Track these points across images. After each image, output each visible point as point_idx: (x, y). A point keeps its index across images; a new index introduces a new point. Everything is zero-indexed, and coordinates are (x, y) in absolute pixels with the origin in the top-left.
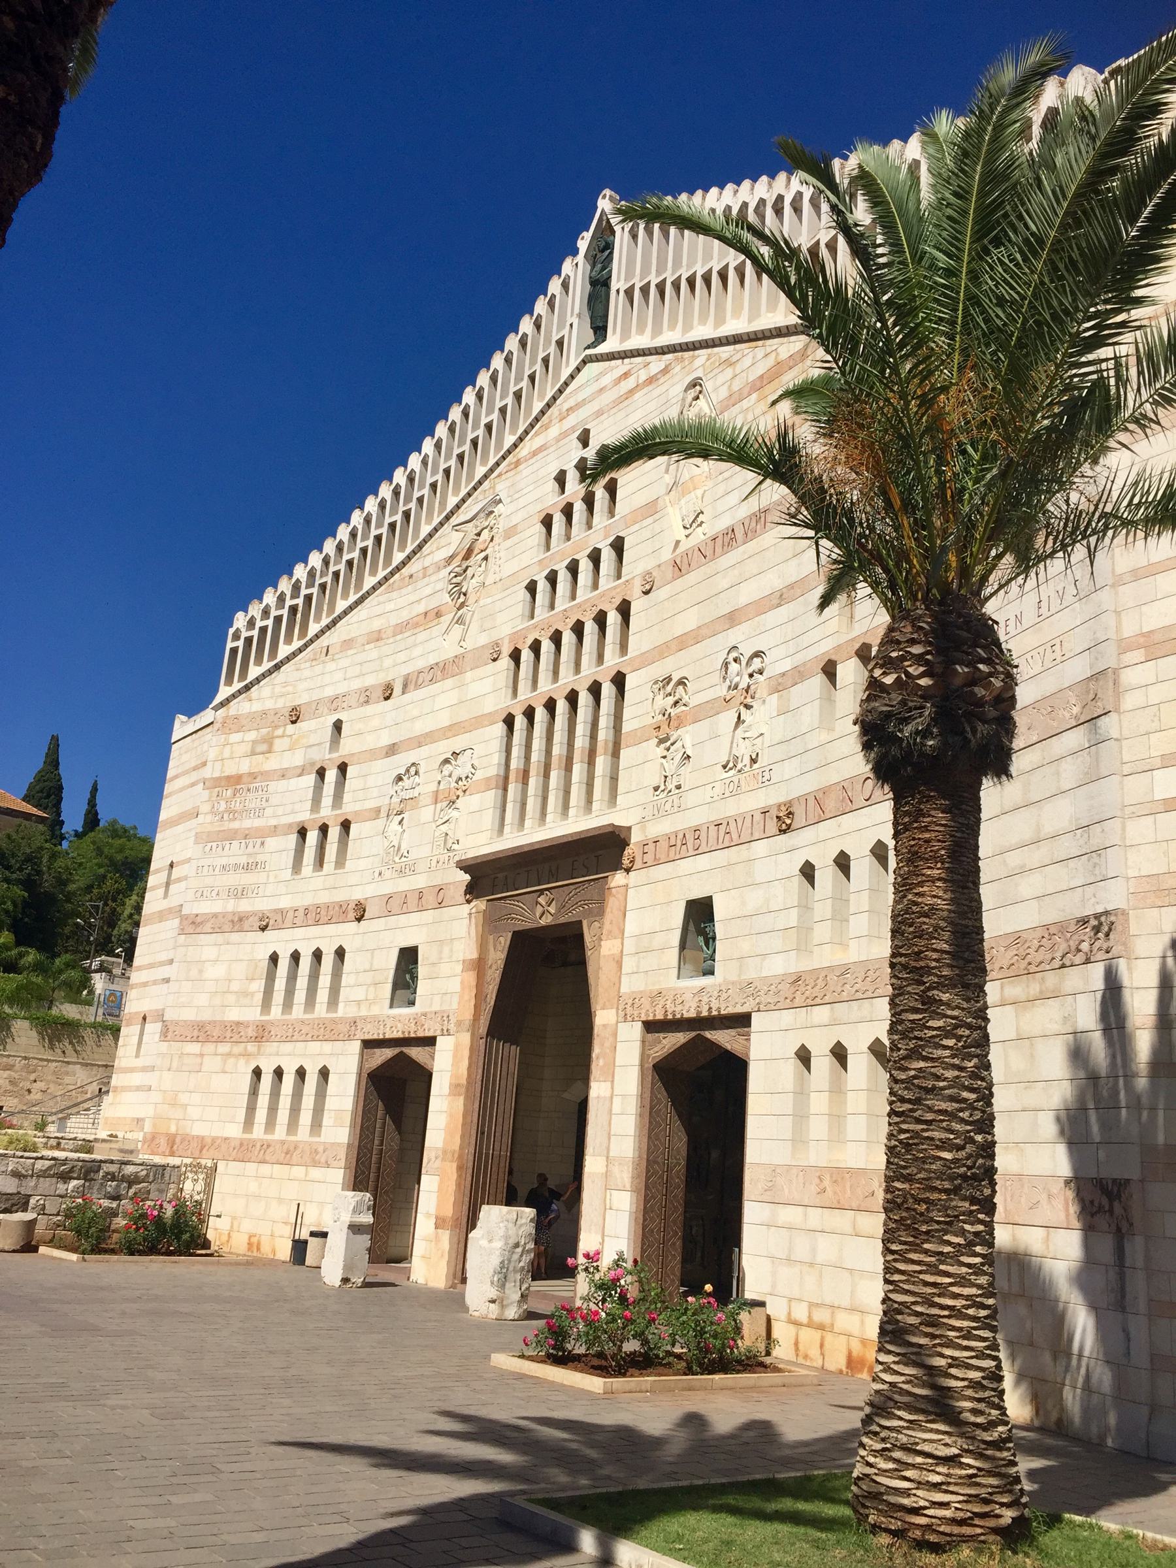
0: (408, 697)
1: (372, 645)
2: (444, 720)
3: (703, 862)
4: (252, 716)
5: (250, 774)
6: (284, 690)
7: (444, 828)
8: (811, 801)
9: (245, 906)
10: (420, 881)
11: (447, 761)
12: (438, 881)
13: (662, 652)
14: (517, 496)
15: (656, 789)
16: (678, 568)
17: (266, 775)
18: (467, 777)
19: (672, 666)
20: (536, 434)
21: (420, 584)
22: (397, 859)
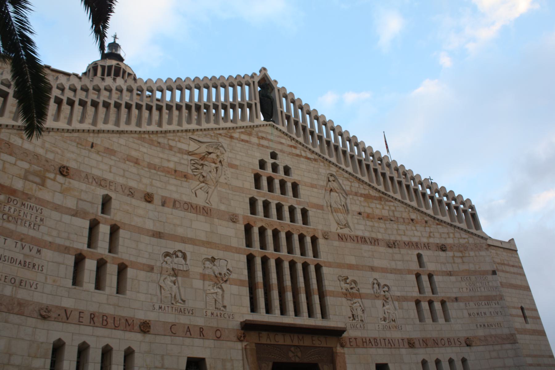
0: (166, 209)
1: (132, 164)
2: (202, 237)
3: (380, 351)
4: (26, 153)
5: (23, 193)
6: (54, 149)
7: (214, 295)
8: (421, 341)
9: (22, 294)
10: (200, 322)
11: (208, 259)
12: (214, 324)
13: (340, 266)
14: (233, 151)
15: (350, 318)
16: (341, 238)
17: (43, 203)
18: (225, 274)
19: (352, 275)
20: (242, 132)
21: (167, 151)
22: (174, 303)
